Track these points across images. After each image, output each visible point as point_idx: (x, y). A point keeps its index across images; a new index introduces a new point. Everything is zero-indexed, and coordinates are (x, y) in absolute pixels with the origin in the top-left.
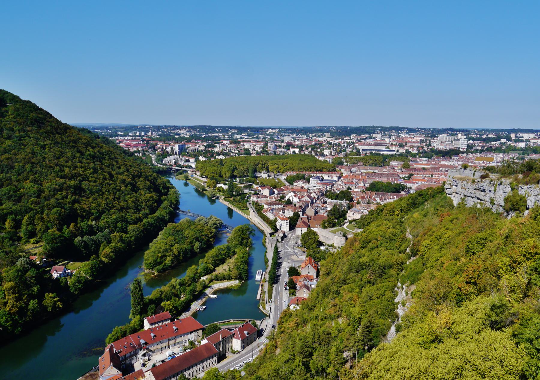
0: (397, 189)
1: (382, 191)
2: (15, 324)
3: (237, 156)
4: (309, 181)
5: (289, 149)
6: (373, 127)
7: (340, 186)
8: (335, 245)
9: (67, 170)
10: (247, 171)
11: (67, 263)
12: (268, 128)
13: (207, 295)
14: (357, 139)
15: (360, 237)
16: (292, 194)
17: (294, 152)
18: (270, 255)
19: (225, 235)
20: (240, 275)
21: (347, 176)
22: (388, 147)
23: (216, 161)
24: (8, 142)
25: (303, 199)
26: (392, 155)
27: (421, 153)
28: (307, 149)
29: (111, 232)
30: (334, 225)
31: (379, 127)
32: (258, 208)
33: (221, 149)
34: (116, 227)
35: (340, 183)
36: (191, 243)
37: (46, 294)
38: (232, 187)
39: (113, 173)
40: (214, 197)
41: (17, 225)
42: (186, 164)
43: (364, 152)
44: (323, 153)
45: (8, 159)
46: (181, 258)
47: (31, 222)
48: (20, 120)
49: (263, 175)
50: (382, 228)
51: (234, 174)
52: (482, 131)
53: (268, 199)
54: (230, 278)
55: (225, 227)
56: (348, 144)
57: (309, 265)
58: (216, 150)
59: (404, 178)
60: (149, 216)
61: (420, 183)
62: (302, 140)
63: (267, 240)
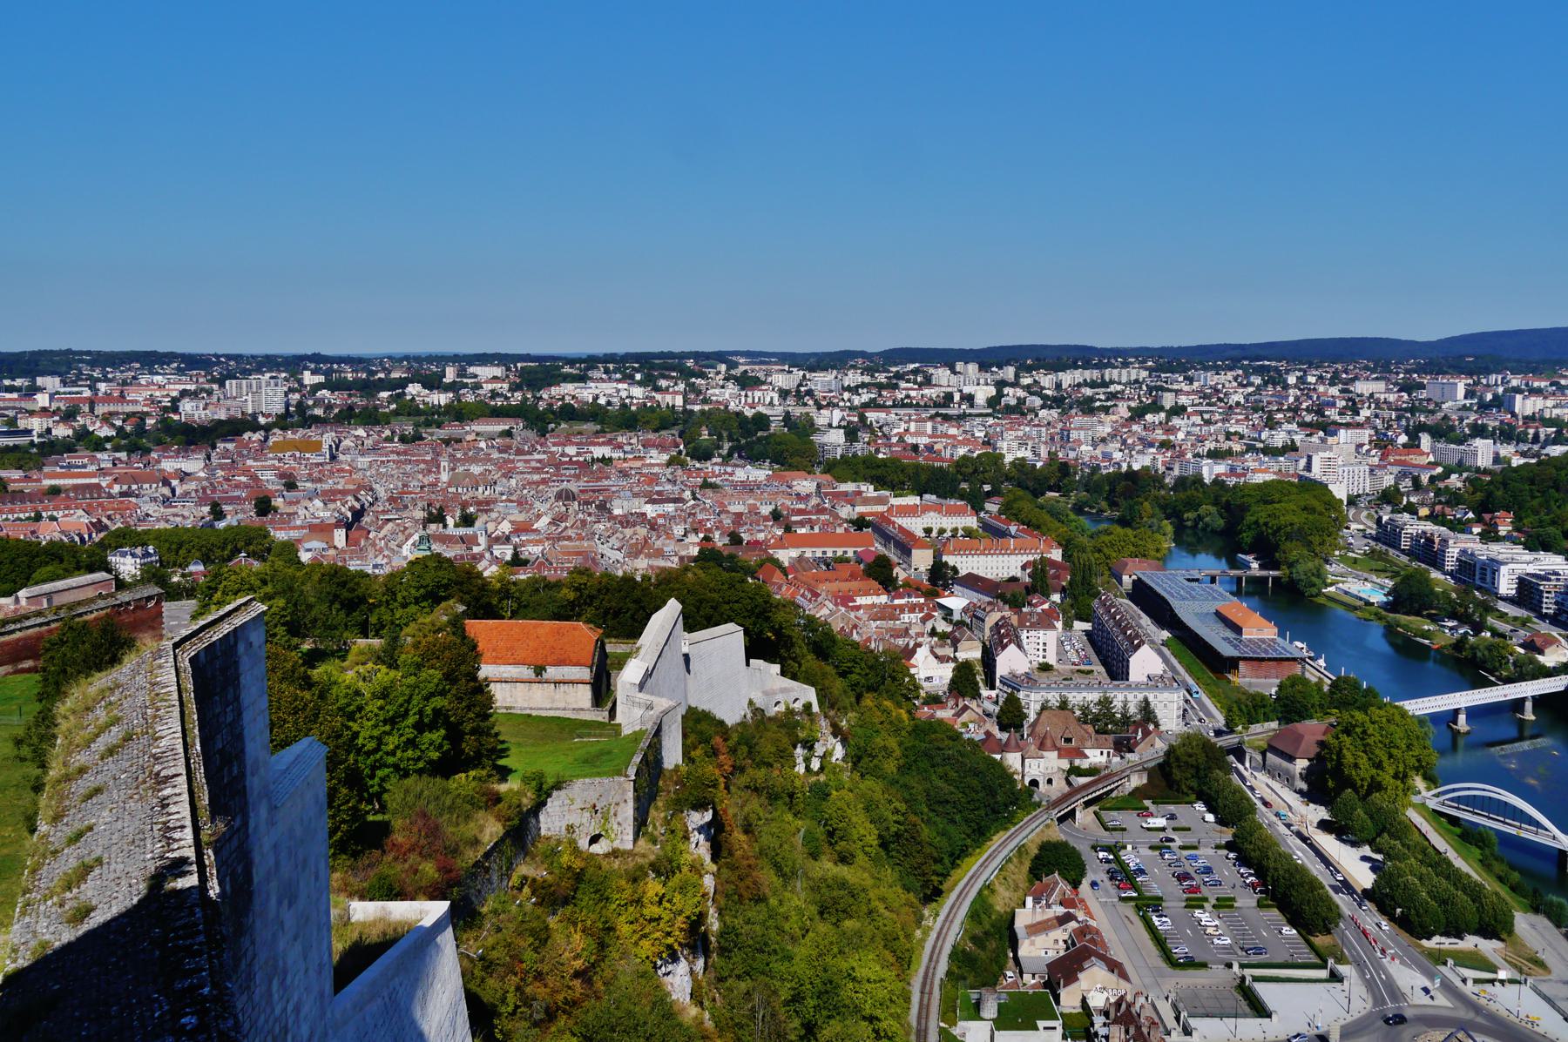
6: (69, 351)
22: (12, 422)
31: (88, 353)
52: (401, 360)
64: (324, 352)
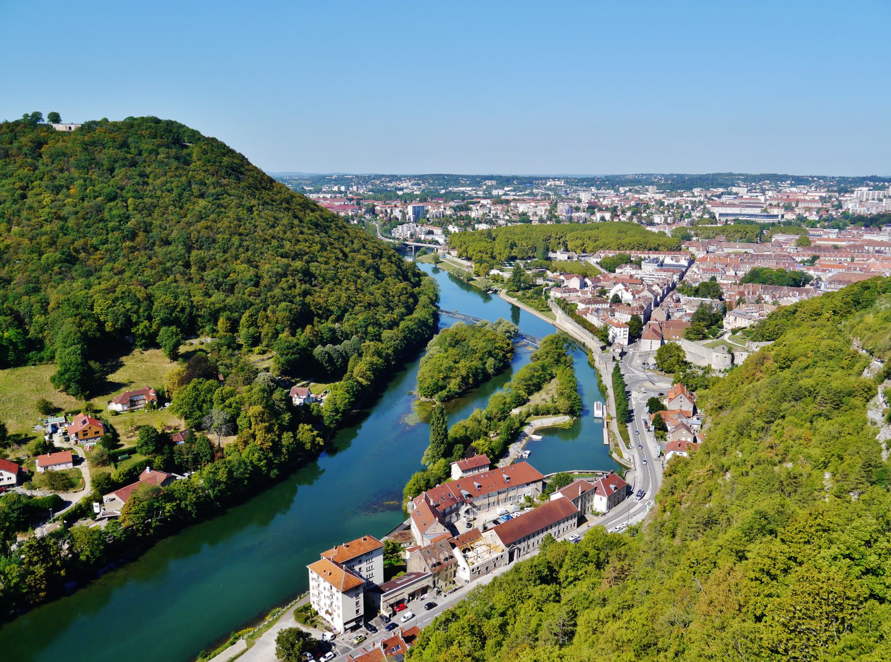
0: (798, 282)
1: (772, 284)
2: (270, 464)
3: (509, 225)
4: (638, 264)
5: (593, 214)
6: (731, 174)
7: (697, 275)
8: (713, 367)
9: (288, 245)
10: (534, 249)
11: (308, 384)
12: (547, 179)
13: (527, 435)
14: (706, 196)
15: (773, 353)
16: (620, 286)
17: (603, 218)
18: (608, 381)
19: (524, 349)
20: (571, 407)
21: (704, 260)
22: (765, 211)
23: (482, 233)
24: (202, 202)
25: (641, 294)
26: (773, 224)
27: (826, 220)
28: (623, 212)
29: (362, 339)
30: (705, 337)
31: (742, 175)
32: (568, 309)
33: (481, 212)
34: (366, 333)
35: (696, 270)
36: (481, 359)
37: (301, 425)
38: (518, 273)
39: (347, 250)
40: (490, 290)
41: (234, 326)
42: (430, 237)
43: (723, 219)
44: (652, 220)
45: (207, 228)
46: (471, 381)
47: (253, 324)
48: (212, 170)
49: (560, 256)
50: (811, 338)
51: (513, 254)
53: (579, 294)
54: (557, 412)
55: (522, 337)
56: (694, 204)
57: (682, 395)
58: (473, 214)
59: (803, 262)
60: (406, 318)
61: (835, 272)
62: (609, 198)
63: (597, 358)
64: (880, 174)
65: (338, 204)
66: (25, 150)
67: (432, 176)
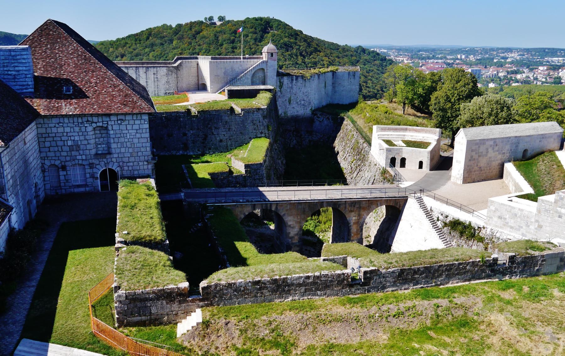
65: (437, 66)
66: (189, 36)
67: (536, 50)
